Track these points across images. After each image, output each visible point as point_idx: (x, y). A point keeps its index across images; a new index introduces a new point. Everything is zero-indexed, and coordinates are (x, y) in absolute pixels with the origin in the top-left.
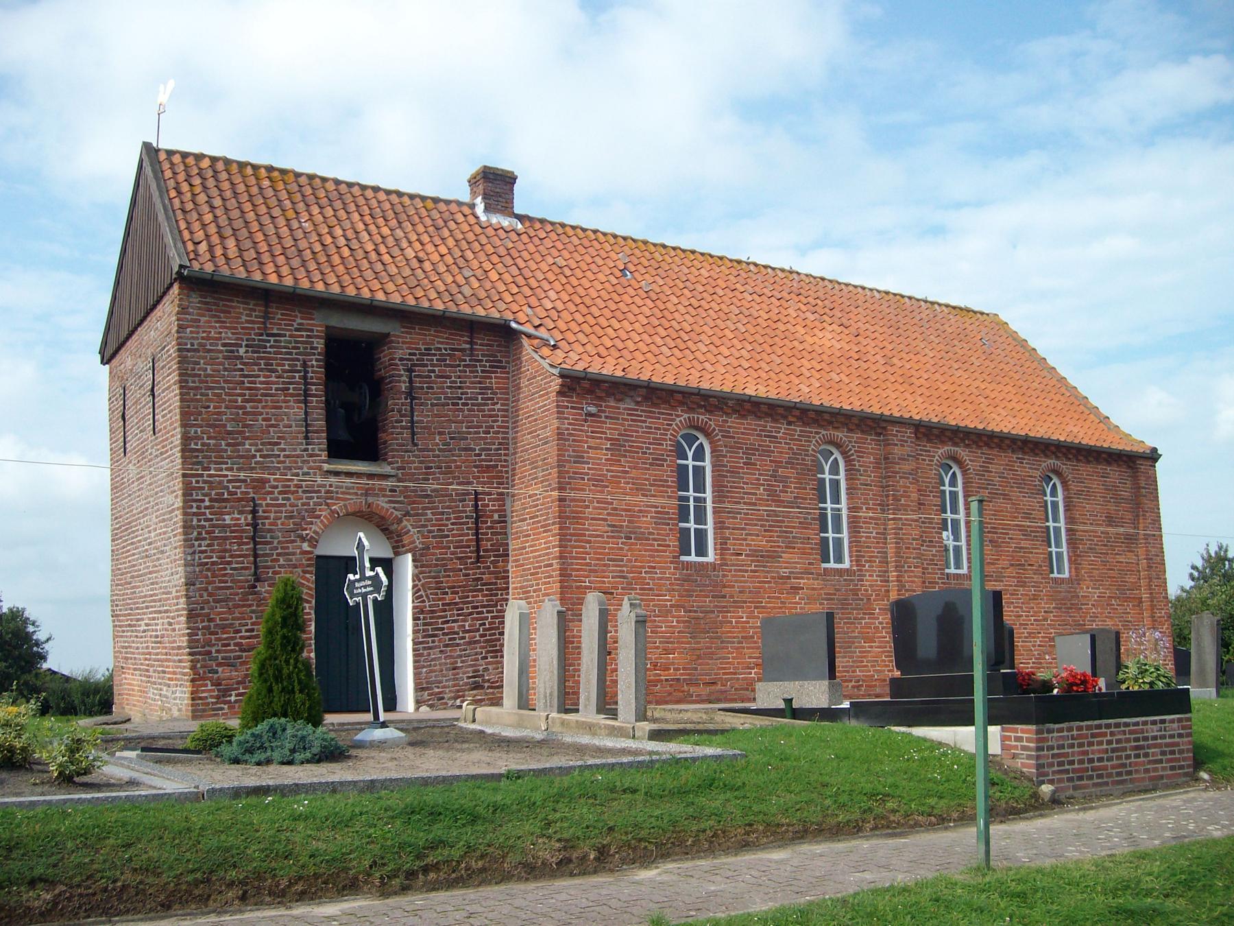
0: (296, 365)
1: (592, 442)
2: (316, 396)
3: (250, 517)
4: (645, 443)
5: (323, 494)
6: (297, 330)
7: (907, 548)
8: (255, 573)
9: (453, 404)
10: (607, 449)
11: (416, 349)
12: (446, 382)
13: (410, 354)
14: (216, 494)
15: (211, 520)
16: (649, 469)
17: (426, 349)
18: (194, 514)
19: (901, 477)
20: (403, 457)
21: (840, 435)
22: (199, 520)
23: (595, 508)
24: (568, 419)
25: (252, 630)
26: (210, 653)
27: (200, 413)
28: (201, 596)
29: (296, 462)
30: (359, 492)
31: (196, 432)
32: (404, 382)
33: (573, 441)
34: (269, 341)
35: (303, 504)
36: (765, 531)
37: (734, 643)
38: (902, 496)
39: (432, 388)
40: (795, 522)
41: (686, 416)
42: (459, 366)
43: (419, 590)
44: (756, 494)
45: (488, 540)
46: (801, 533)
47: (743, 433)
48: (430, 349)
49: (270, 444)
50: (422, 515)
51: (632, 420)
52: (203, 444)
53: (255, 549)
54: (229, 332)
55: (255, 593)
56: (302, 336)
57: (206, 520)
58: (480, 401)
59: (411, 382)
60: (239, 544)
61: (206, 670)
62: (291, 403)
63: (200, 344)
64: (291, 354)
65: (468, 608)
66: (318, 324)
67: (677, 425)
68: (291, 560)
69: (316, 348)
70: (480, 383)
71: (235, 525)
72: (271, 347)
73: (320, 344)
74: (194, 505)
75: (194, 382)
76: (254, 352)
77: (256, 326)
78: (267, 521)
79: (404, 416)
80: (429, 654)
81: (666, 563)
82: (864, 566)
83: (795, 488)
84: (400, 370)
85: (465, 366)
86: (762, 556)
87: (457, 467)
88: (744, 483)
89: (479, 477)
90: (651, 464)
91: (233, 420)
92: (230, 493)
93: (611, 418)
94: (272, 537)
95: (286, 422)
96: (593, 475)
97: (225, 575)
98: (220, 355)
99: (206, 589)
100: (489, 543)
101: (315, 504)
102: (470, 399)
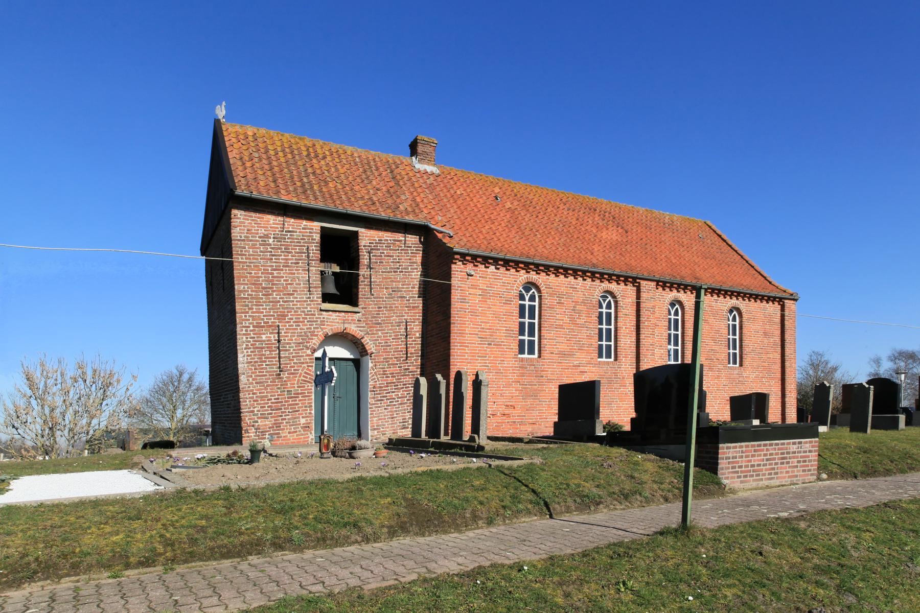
0: (303, 249)
1: (471, 291)
3: (276, 335)
5: (319, 323)
6: (303, 229)
8: (280, 367)
9: (394, 272)
10: (479, 295)
11: (374, 240)
12: (390, 259)
13: (370, 243)
14: (257, 323)
16: (503, 306)
17: (379, 240)
18: (244, 334)
19: (646, 310)
20: (365, 302)
21: (613, 287)
22: (247, 338)
23: (471, 328)
24: (458, 278)
25: (278, 399)
26: (253, 411)
27: (246, 277)
28: (248, 380)
29: (303, 305)
30: (340, 321)
31: (244, 288)
32: (367, 259)
33: (461, 290)
34: (287, 235)
35: (307, 329)
36: (567, 340)
41: (525, 276)
42: (398, 250)
43: (373, 375)
44: (563, 320)
45: (412, 348)
46: (588, 342)
49: (288, 294)
51: (495, 279)
52: (248, 295)
53: (279, 354)
54: (263, 230)
55: (280, 378)
56: (307, 232)
57: (251, 338)
58: (410, 270)
59: (370, 259)
60: (270, 351)
61: (252, 421)
62: (300, 271)
63: (245, 237)
64: (300, 242)
65: (400, 385)
66: (316, 226)
67: (520, 281)
68: (300, 360)
69: (315, 239)
70: (410, 259)
71: (268, 341)
72: (288, 238)
73: (317, 237)
74: (244, 329)
75: (242, 259)
76: (278, 241)
77: (279, 226)
78: (287, 338)
79: (367, 278)
80: (378, 410)
81: (511, 358)
84: (364, 252)
85: (401, 250)
87: (395, 307)
89: (408, 313)
90: (504, 303)
91: (266, 281)
92: (264, 323)
93: (483, 277)
94: (289, 347)
95: (297, 282)
97: (262, 369)
98: (258, 243)
99: (251, 376)
100: (413, 349)
101: (314, 328)
102: (405, 269)
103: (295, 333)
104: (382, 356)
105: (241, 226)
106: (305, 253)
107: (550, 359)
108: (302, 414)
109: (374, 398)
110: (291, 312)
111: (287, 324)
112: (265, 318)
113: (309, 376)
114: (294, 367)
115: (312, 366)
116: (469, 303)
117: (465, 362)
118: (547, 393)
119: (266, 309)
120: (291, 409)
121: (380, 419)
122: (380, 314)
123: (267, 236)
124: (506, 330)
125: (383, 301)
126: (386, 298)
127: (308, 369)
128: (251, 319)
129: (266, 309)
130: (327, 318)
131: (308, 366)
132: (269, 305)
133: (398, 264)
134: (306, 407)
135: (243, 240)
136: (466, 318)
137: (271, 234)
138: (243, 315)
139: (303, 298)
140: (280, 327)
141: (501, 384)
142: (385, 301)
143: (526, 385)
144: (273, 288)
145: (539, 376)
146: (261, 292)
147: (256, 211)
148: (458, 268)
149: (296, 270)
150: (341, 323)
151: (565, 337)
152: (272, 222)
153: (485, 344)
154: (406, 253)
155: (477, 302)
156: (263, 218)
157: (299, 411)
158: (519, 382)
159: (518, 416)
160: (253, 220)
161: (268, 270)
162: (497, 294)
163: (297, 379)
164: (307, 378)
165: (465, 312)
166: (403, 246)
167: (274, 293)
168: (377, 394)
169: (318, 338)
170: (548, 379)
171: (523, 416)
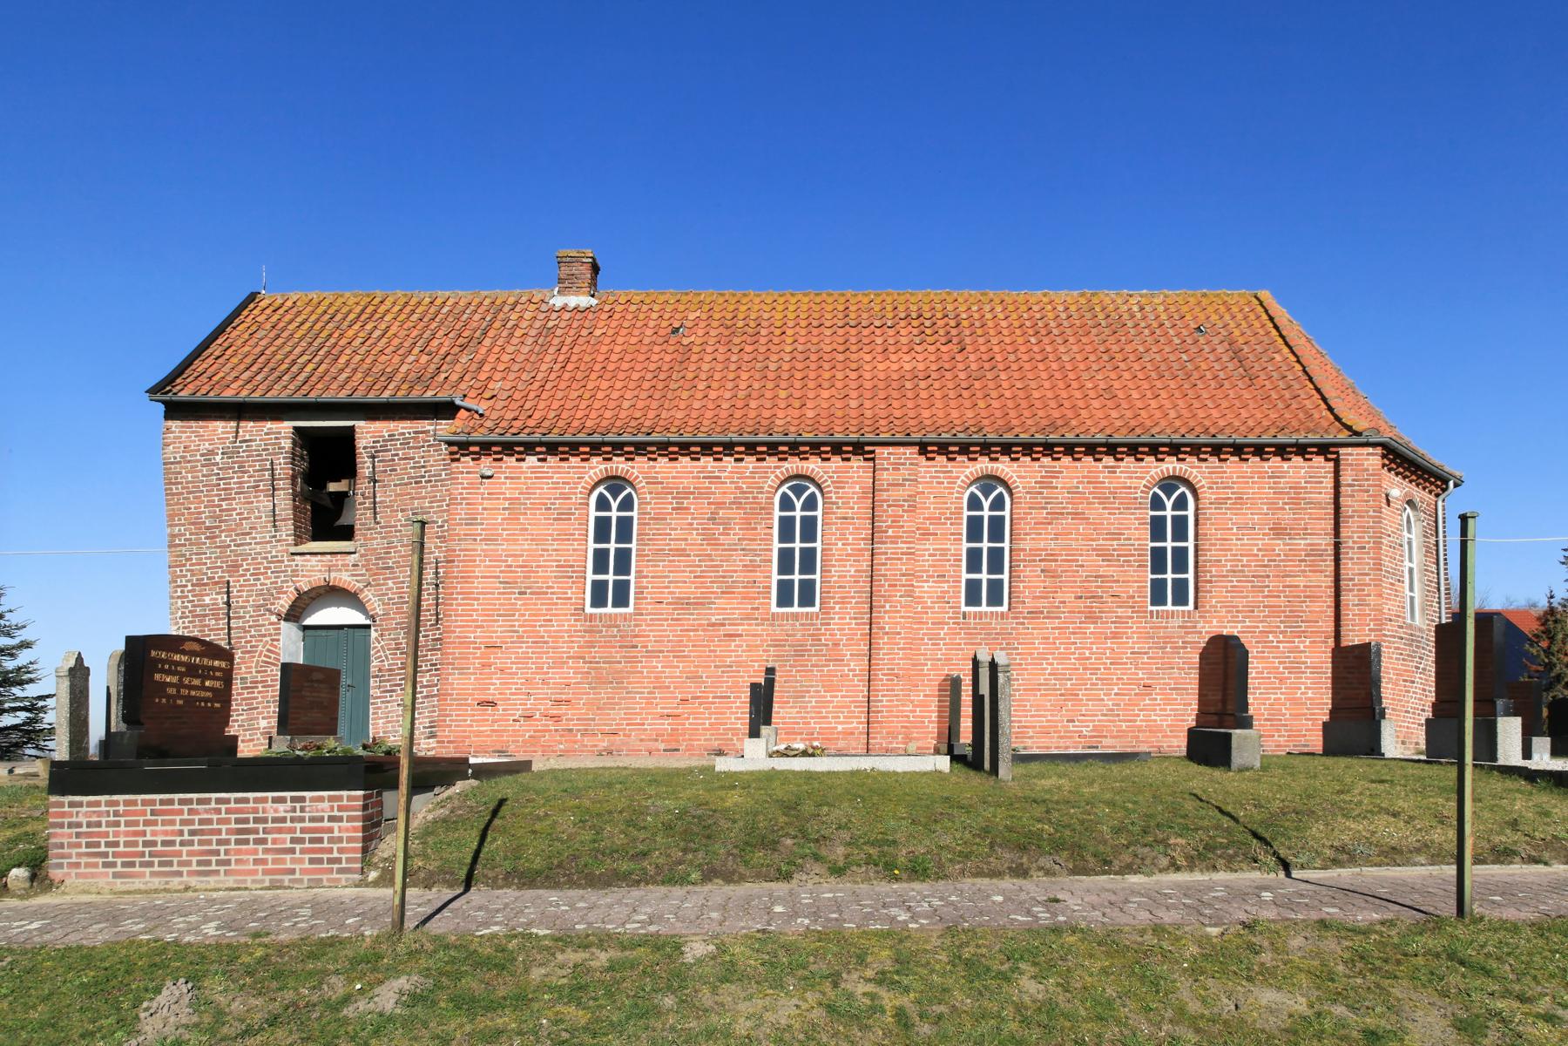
2: (284, 489)
3: (225, 596)
4: (550, 499)
5: (289, 573)
6: (267, 434)
7: (890, 586)
10: (504, 509)
11: (380, 437)
14: (197, 580)
15: (193, 601)
16: (553, 525)
17: (389, 436)
18: (179, 597)
19: (889, 506)
20: (365, 535)
21: (812, 466)
22: (183, 602)
23: (485, 566)
24: (462, 484)
27: (183, 514)
31: (180, 530)
33: (467, 504)
34: (242, 447)
35: (271, 583)
36: (695, 577)
37: (643, 693)
38: (890, 527)
39: (396, 470)
40: (738, 566)
41: (603, 467)
42: (423, 447)
43: (379, 651)
44: (686, 540)
47: (673, 478)
48: (394, 435)
49: (243, 534)
50: (383, 585)
51: (536, 478)
53: (229, 623)
54: (207, 444)
56: (271, 439)
57: (188, 602)
59: (374, 467)
60: (216, 620)
62: (262, 498)
63: (181, 457)
66: (287, 427)
69: (284, 448)
71: (213, 604)
72: (243, 451)
73: (287, 444)
74: (179, 590)
75: (177, 489)
79: (368, 498)
81: (566, 615)
82: (834, 608)
83: (740, 529)
85: (428, 446)
86: (687, 604)
88: (671, 529)
90: (555, 519)
91: (211, 517)
92: (208, 578)
93: (512, 478)
96: (486, 535)
101: (282, 582)
102: (434, 476)
103: (252, 591)
104: (393, 619)
105: (175, 443)
106: (268, 470)
107: (655, 614)
108: (263, 713)
109: (379, 687)
110: (247, 559)
111: (242, 579)
112: (209, 571)
113: (273, 656)
114: (251, 641)
115: (278, 640)
116: (483, 524)
117: (471, 626)
118: (645, 677)
119: (210, 558)
120: (246, 705)
121: (389, 722)
122: (390, 553)
123: (212, 452)
124: (557, 566)
125: (396, 531)
126: (401, 526)
127: (272, 645)
128: (189, 574)
129: (210, 558)
130: (302, 566)
131: (272, 640)
132: (216, 552)
133: (423, 470)
134: (268, 702)
135: (180, 462)
136: (477, 550)
137: (218, 449)
138: (178, 569)
139: (265, 537)
140: (231, 584)
141: (544, 663)
142: (401, 531)
143: (597, 663)
144: (221, 526)
145: (626, 647)
146: (203, 534)
147: (197, 418)
148: (463, 467)
149: (255, 497)
150: (325, 571)
151: (690, 572)
152: (220, 430)
153: (515, 593)
154: (437, 451)
155: (499, 521)
156: (208, 427)
157: (258, 708)
158: (584, 658)
159: (578, 719)
160: (193, 432)
161: (214, 501)
162: (540, 504)
163: (255, 659)
164: (270, 657)
165: (475, 540)
166: (432, 439)
167: (223, 535)
168: (384, 681)
169: (288, 597)
170: (647, 652)
171: (588, 720)
